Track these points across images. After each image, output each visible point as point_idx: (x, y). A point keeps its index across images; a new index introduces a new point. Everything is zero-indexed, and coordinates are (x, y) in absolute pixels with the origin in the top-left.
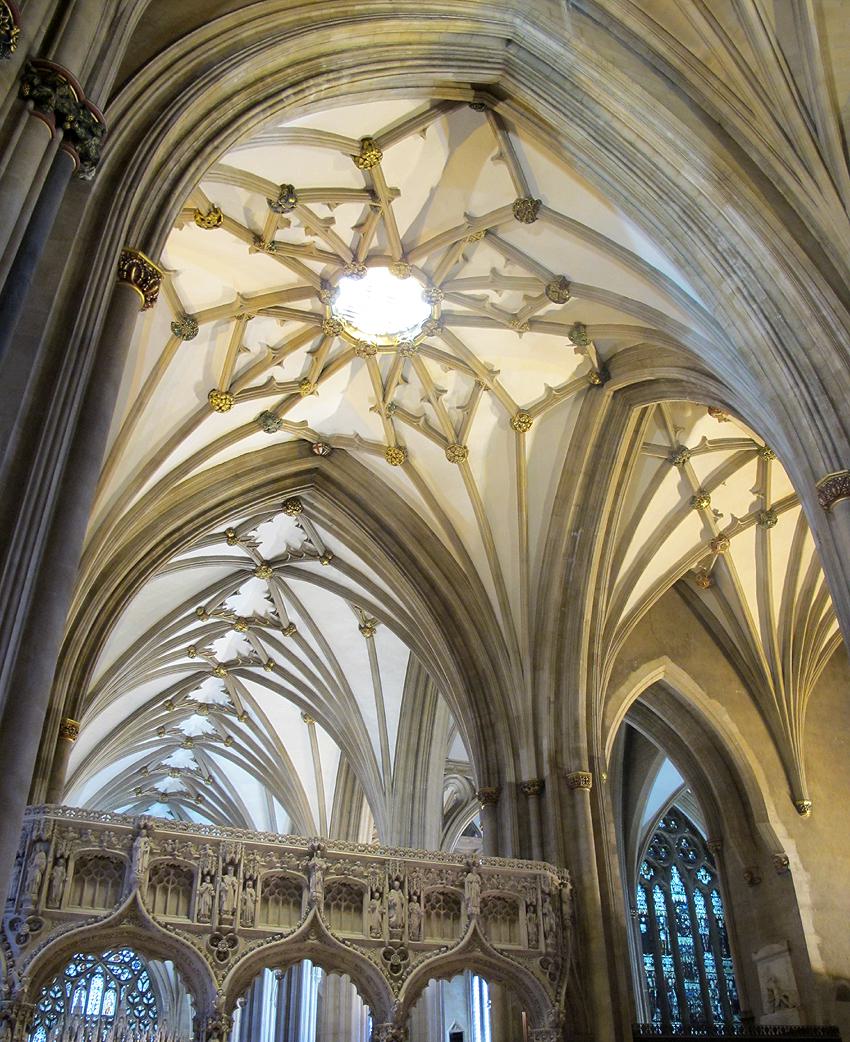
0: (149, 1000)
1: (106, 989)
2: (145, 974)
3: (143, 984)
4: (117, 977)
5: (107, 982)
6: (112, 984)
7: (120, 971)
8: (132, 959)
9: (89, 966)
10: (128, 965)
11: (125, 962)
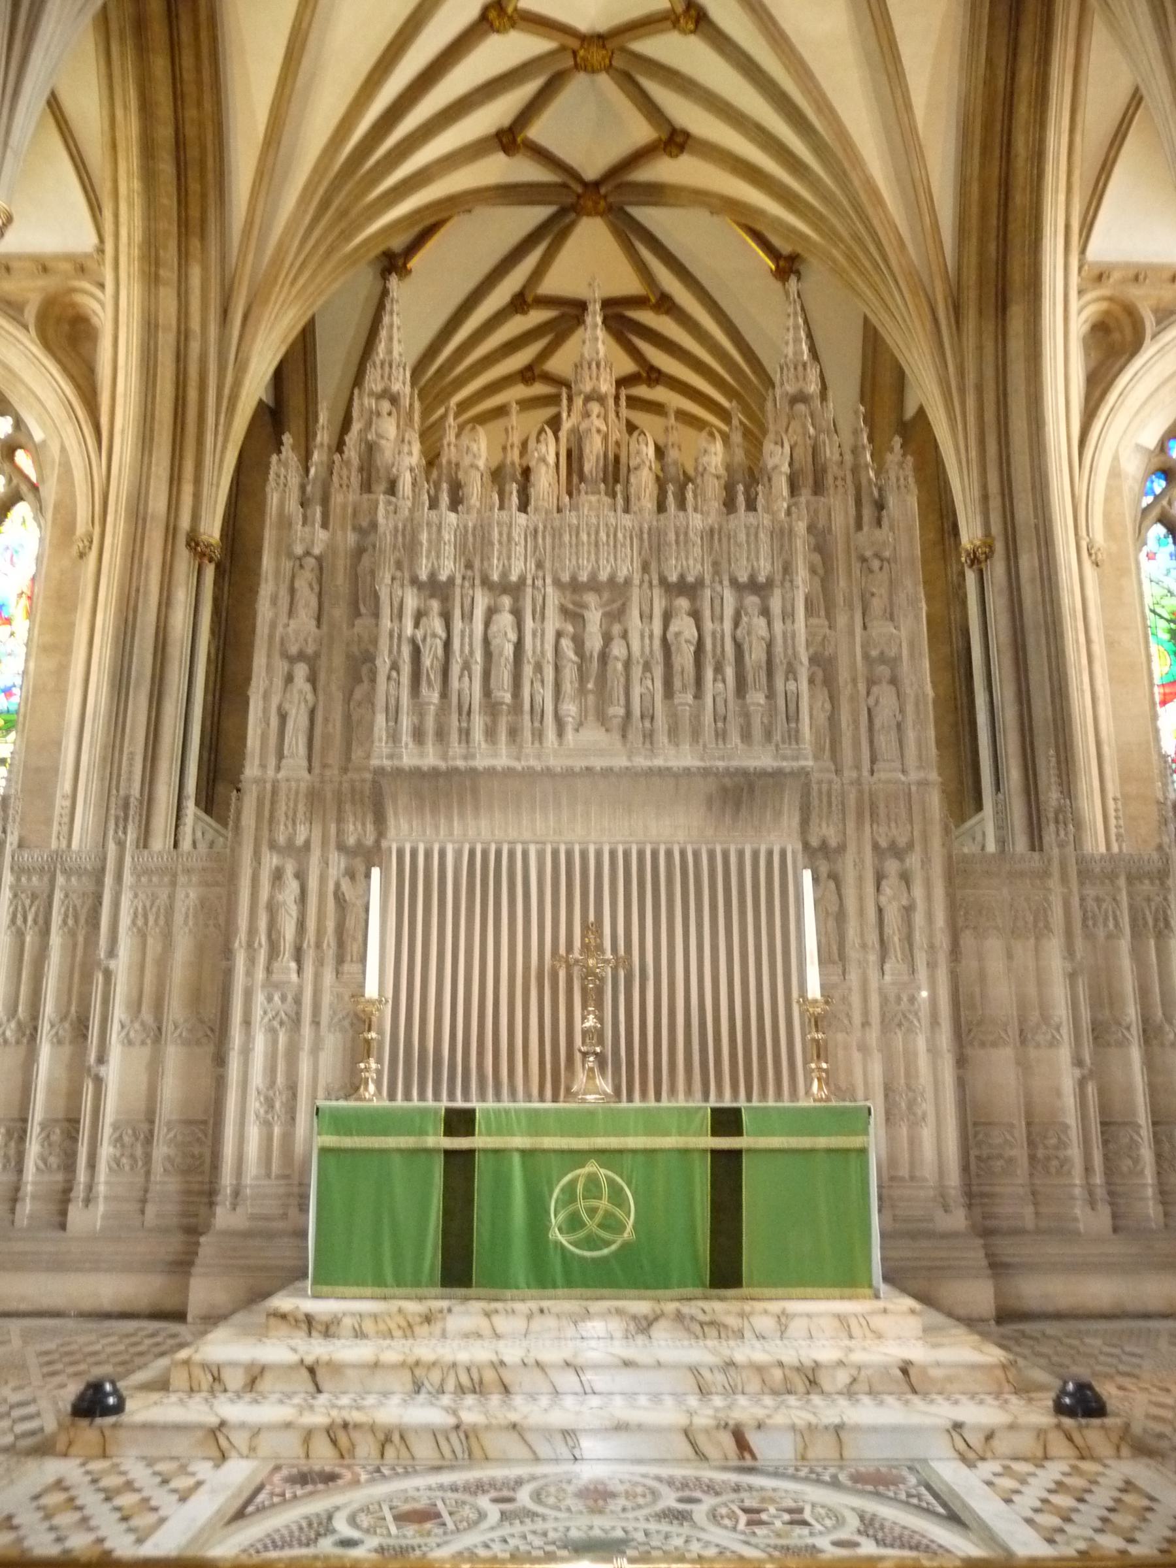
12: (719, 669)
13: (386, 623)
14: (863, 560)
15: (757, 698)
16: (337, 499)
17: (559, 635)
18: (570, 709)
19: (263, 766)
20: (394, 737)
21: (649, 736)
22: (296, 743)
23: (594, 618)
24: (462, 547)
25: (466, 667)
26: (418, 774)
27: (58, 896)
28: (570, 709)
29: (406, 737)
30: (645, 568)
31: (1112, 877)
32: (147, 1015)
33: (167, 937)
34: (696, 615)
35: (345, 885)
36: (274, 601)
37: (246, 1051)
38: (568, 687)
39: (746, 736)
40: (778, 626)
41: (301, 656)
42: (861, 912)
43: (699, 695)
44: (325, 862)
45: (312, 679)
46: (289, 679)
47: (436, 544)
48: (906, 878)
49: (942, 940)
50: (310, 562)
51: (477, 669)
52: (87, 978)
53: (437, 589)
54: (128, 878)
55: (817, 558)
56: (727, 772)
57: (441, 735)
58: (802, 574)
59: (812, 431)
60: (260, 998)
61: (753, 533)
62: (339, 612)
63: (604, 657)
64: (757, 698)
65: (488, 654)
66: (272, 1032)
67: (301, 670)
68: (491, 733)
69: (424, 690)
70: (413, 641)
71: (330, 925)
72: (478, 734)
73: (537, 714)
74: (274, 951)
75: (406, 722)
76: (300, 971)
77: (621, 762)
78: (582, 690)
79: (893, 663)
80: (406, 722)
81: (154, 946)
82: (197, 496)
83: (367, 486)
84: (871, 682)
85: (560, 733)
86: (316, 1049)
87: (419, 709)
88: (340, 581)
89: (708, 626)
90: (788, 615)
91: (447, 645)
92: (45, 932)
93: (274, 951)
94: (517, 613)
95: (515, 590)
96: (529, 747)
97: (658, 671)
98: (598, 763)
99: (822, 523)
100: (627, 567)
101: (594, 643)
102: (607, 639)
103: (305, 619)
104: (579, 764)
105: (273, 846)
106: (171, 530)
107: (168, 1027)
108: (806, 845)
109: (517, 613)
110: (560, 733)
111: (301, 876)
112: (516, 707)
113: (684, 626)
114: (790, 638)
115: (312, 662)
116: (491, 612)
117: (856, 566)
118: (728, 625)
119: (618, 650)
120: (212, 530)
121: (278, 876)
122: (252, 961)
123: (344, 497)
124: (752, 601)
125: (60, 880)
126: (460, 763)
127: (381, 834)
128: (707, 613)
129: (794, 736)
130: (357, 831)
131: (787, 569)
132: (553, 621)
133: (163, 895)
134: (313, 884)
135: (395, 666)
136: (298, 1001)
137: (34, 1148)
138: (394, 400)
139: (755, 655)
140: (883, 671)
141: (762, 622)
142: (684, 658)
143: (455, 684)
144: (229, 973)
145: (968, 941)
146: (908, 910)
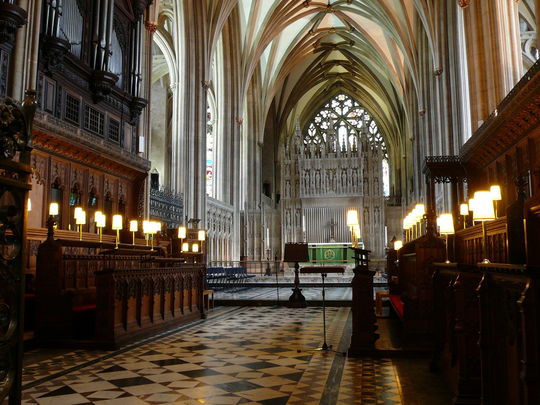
0: (378, 139)
1: (349, 135)
2: (373, 123)
3: (373, 129)
4: (355, 127)
5: (349, 131)
6: (353, 131)
10: (360, 118)
11: (358, 117)
12: (350, 182)
13: (301, 176)
15: (355, 186)
17: (326, 177)
18: (328, 189)
19: (283, 197)
20: (303, 193)
21: (340, 192)
22: (288, 193)
23: (331, 174)
24: (311, 164)
25: (313, 183)
26: (306, 198)
28: (328, 189)
30: (339, 166)
33: (271, 222)
34: (346, 173)
35: (297, 214)
36: (283, 172)
37: (284, 238)
39: (354, 192)
40: (359, 175)
41: (288, 180)
42: (372, 216)
43: (347, 186)
44: (293, 211)
45: (290, 184)
46: (286, 184)
47: (307, 164)
48: (379, 211)
49: (384, 220)
50: (288, 165)
51: (314, 183)
52: (260, 228)
53: (308, 171)
54: (265, 214)
56: (351, 197)
57: (309, 193)
58: (362, 166)
60: (285, 230)
61: (354, 160)
62: (293, 173)
63: (333, 180)
64: (355, 186)
65: (316, 181)
66: (287, 235)
67: (288, 182)
68: (317, 192)
70: (305, 179)
72: (315, 192)
73: (323, 189)
75: (304, 191)
79: (377, 178)
80: (304, 191)
82: (259, 134)
83: (296, 153)
84: (375, 181)
85: (327, 192)
87: (306, 189)
88: (293, 167)
89: (348, 175)
90: (360, 173)
91: (310, 179)
92: (254, 222)
94: (320, 174)
96: (322, 195)
97: (341, 182)
98: (332, 196)
100: (336, 166)
101: (331, 178)
102: (333, 178)
103: (288, 174)
104: (329, 197)
106: (255, 142)
108: (364, 207)
109: (320, 174)
110: (327, 192)
112: (320, 188)
113: (344, 175)
114: (360, 176)
115: (290, 181)
116: (316, 174)
118: (351, 175)
119: (335, 179)
120: (262, 141)
121: (287, 213)
122: (284, 225)
123: (293, 155)
124: (355, 171)
126: (313, 197)
127: (301, 207)
128: (348, 173)
129: (361, 191)
130: (298, 206)
131: (360, 166)
132: (325, 175)
133: (270, 217)
135: (302, 183)
136: (291, 231)
137: (255, 252)
138: (299, 137)
139: (355, 180)
140: (376, 180)
142: (344, 180)
144: (281, 227)
145: (388, 220)
146: (379, 216)
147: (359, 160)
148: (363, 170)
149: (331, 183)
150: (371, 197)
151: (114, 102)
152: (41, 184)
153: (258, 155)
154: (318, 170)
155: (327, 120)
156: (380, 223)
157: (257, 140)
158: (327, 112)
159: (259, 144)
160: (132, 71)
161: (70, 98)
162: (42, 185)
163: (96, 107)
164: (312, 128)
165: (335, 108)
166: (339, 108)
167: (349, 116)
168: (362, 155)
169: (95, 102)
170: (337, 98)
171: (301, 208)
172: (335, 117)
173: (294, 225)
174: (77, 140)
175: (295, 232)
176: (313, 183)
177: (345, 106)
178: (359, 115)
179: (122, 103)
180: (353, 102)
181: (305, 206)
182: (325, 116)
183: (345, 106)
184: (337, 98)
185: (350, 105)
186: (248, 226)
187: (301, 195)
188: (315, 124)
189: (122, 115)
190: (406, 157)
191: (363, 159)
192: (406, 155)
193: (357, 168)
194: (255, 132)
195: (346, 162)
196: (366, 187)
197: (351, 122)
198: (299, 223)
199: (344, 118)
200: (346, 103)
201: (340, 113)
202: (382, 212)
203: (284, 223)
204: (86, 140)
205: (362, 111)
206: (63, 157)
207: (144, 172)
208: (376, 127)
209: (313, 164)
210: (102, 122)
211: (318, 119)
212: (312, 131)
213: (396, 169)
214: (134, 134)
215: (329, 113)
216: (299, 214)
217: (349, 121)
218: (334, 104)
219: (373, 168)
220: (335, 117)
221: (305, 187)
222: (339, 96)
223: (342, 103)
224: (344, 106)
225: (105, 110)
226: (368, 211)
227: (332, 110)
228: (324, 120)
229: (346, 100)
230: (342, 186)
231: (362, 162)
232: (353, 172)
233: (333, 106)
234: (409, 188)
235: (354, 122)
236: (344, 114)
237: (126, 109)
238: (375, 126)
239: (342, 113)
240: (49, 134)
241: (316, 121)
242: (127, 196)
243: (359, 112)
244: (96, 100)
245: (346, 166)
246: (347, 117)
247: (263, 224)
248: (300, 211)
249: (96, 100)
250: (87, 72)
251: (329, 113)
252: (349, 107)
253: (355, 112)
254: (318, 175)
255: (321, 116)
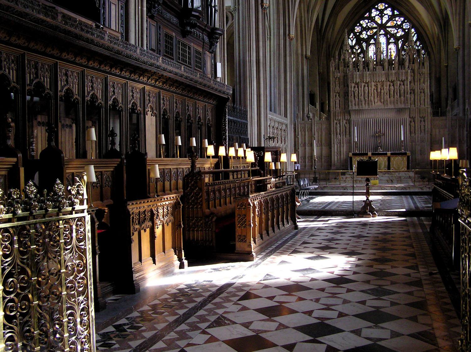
0: (418, 46)
1: (388, 43)
4: (394, 36)
6: (392, 40)
7: (396, 31)
8: (403, 22)
9: (375, 30)
12: (397, 93)
13: (350, 89)
14: (419, 73)
15: (402, 98)
16: (340, 68)
17: (374, 89)
18: (376, 100)
20: (352, 105)
21: (387, 104)
22: (338, 105)
23: (379, 87)
25: (361, 95)
26: (355, 110)
27: (306, 127)
29: (353, 105)
31: (456, 120)
32: (320, 142)
33: (321, 132)
35: (346, 124)
36: (333, 85)
38: (376, 97)
40: (406, 87)
44: (343, 121)
45: (339, 96)
46: (336, 96)
47: (356, 78)
48: (424, 121)
51: (363, 95)
53: (357, 84)
55: (412, 74)
56: (398, 108)
57: (358, 104)
59: (412, 52)
60: (335, 140)
62: (342, 86)
63: (380, 92)
64: (402, 98)
67: (337, 95)
68: (365, 104)
69: (356, 98)
71: (344, 130)
72: (363, 104)
74: (337, 134)
75: (353, 103)
76: (340, 137)
77: (383, 107)
78: (377, 97)
79: (424, 90)
81: (320, 133)
83: (345, 67)
85: (375, 103)
86: (343, 147)
89: (395, 87)
90: (407, 85)
93: (337, 134)
94: (368, 86)
95: (367, 83)
97: (388, 94)
99: (413, 68)
101: (379, 90)
103: (338, 88)
105: (335, 120)
107: (323, 144)
108: (410, 117)
109: (368, 86)
110: (375, 103)
111: (340, 124)
113: (392, 88)
115: (339, 93)
116: (364, 86)
117: (419, 75)
118: (398, 87)
119: (382, 91)
121: (336, 123)
122: (334, 135)
125: (306, 125)
126: (361, 109)
127: (350, 118)
130: (347, 117)
131: (407, 78)
132: (373, 87)
133: (321, 126)
134: (341, 125)
135: (351, 95)
136: (340, 140)
137: (307, 160)
141: (403, 86)
142: (392, 93)
143: (360, 97)
147: (407, 73)
148: (410, 82)
149: (379, 94)
150: (417, 108)
151: (197, 34)
152: (154, 116)
153: (305, 68)
154: (366, 83)
155: (367, 29)
156: (426, 132)
157: (304, 53)
158: (367, 21)
159: (306, 57)
160: (209, 3)
161: (166, 35)
162: (155, 117)
163: (185, 41)
164: (352, 38)
165: (374, 17)
166: (378, 17)
167: (389, 24)
168: (409, 67)
169: (184, 36)
170: (376, 7)
171: (350, 119)
172: (375, 25)
173: (343, 135)
174: (181, 76)
175: (344, 142)
176: (361, 95)
177: (385, 15)
178: (399, 23)
179: (203, 34)
180: (393, 11)
181: (353, 117)
182: (364, 26)
183: (385, 15)
184: (376, 7)
185: (390, 14)
186: (300, 137)
187: (350, 107)
188: (355, 34)
189: (203, 45)
190: (448, 65)
191: (409, 71)
192: (448, 63)
193: (404, 80)
194: (302, 45)
195: (393, 74)
196: (412, 99)
197: (391, 31)
198: (348, 133)
199: (382, 26)
200: (385, 12)
201: (379, 22)
202: (428, 122)
203: (334, 133)
204: (187, 75)
205: (402, 19)
206: (168, 91)
207: (227, 97)
208: (416, 35)
209: (362, 76)
210: (190, 53)
211: (358, 29)
212: (352, 41)
213: (435, 77)
214: (212, 61)
215: (369, 22)
216: (348, 125)
217: (389, 29)
218: (374, 13)
219: (420, 80)
220: (375, 25)
221: (354, 99)
222: (379, 4)
223: (381, 12)
224: (383, 15)
225: (191, 42)
226: (414, 121)
227: (372, 19)
228: (364, 29)
229: (386, 8)
230: (390, 97)
231: (409, 74)
232: (400, 84)
233: (373, 15)
234: (451, 96)
235: (393, 31)
236: (384, 23)
237: (206, 39)
238: (415, 34)
239: (382, 22)
240: (144, 67)
241: (356, 31)
242: (212, 119)
243: (399, 20)
244: (185, 34)
245: (393, 78)
246: (387, 25)
247: (314, 135)
248: (349, 122)
249: (185, 34)
250: (178, 10)
251: (369, 22)
252: (389, 16)
253: (395, 20)
254: (366, 88)
255: (361, 25)
